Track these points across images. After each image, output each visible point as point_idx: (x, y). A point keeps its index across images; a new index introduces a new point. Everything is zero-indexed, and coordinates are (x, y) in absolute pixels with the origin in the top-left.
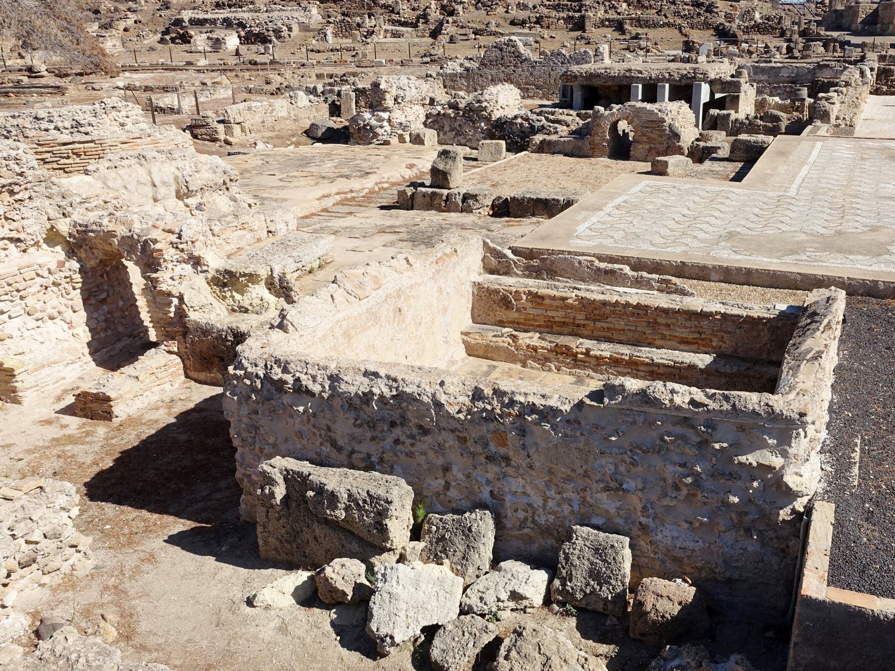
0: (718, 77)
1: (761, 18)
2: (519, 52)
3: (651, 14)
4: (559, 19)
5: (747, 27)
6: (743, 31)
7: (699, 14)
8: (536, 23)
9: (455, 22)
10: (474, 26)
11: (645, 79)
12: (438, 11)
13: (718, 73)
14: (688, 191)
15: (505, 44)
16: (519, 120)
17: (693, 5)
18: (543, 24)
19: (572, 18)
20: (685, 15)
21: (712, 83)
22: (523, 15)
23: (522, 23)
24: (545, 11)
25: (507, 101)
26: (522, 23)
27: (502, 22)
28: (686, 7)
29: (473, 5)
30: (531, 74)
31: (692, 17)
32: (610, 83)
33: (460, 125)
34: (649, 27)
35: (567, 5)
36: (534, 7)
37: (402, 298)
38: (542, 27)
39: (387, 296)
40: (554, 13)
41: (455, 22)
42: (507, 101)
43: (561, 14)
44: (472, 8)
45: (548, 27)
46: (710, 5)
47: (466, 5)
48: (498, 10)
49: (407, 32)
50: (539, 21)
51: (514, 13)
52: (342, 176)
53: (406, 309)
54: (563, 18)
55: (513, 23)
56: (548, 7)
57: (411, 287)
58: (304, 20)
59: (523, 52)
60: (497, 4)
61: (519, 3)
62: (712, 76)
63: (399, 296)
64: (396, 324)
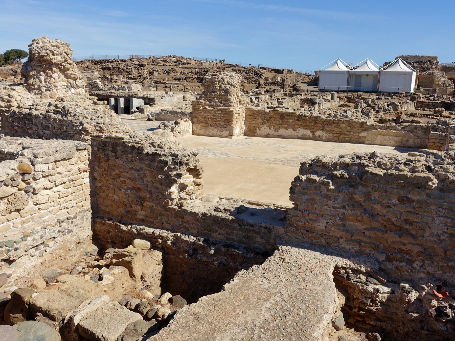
1: (281, 80)
4: (194, 78)
5: (270, 83)
6: (269, 85)
7: (253, 78)
8: (185, 79)
9: (151, 78)
10: (156, 80)
12: (148, 74)
17: (255, 74)
18: (188, 80)
19: (199, 78)
20: (247, 78)
23: (179, 79)
24: (190, 74)
26: (179, 79)
27: (171, 79)
28: (251, 75)
29: (163, 72)
31: (250, 79)
35: (201, 73)
36: (188, 73)
38: (187, 81)
41: (151, 78)
44: (162, 73)
45: (190, 81)
46: (261, 74)
47: (160, 72)
48: (171, 74)
49: (131, 82)
50: (186, 79)
51: (178, 75)
54: (196, 78)
55: (175, 79)
56: (194, 73)
58: (89, 76)
60: (172, 72)
61: (181, 72)
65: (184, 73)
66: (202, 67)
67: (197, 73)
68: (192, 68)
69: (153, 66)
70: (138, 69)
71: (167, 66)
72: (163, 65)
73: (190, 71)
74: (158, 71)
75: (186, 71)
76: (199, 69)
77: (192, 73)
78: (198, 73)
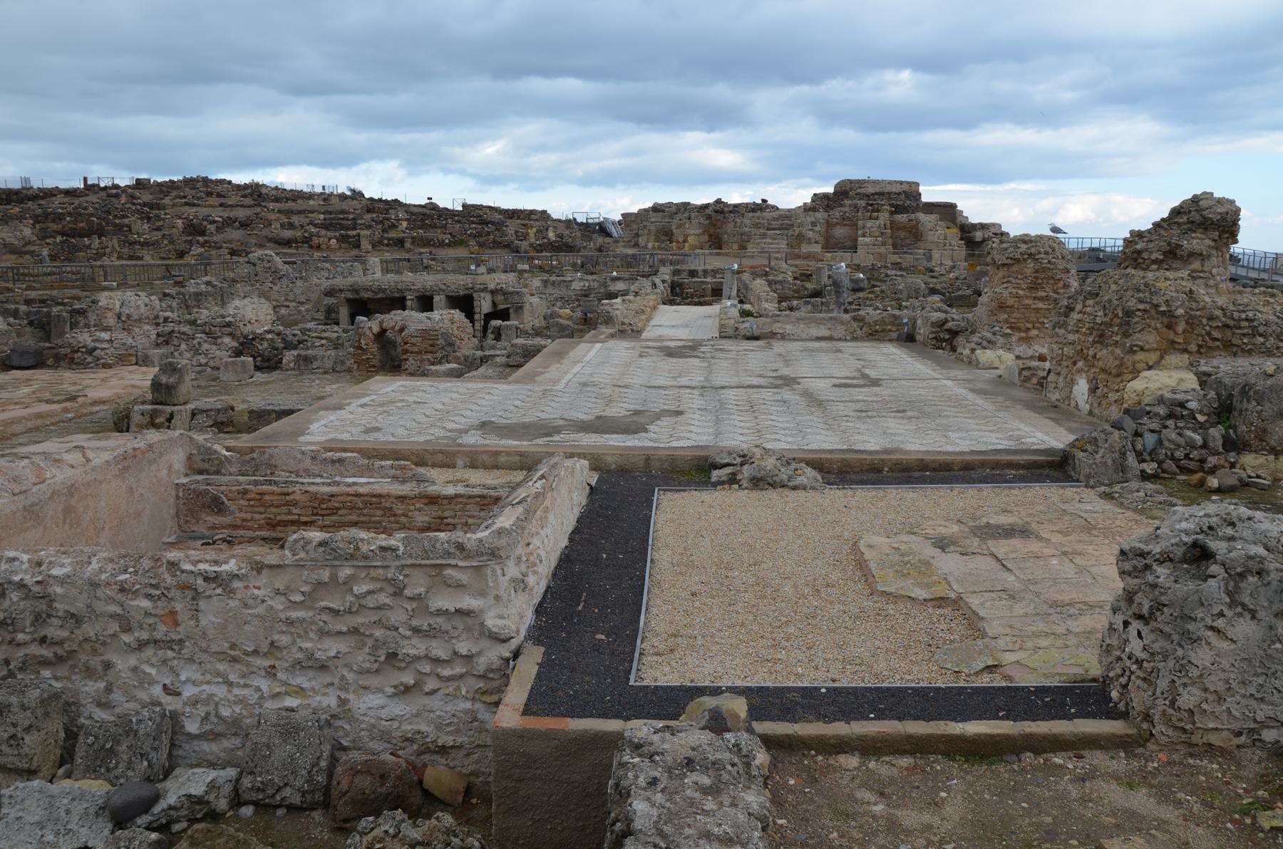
0: (498, 287)
2: (276, 268)
3: (436, 235)
8: (303, 242)
11: (418, 291)
13: (498, 284)
14: (446, 390)
15: (259, 259)
16: (270, 336)
21: (493, 292)
22: (288, 234)
25: (257, 315)
30: (292, 291)
32: (381, 295)
33: (199, 343)
34: (434, 245)
35: (340, 224)
37: (76, 497)
38: (311, 247)
39: (53, 493)
40: (323, 232)
42: (257, 315)
43: (333, 234)
52: (40, 401)
53: (81, 509)
54: (335, 237)
57: (89, 485)
59: (281, 267)
62: (492, 286)
63: (72, 495)
64: (67, 527)
65: (291, 226)
66: (330, 209)
67: (327, 226)
68: (304, 211)
69: (194, 209)
70: (149, 219)
71: (231, 206)
72: (221, 205)
73: (307, 220)
74: (214, 222)
75: (295, 219)
76: (324, 213)
77: (311, 223)
78: (331, 225)
